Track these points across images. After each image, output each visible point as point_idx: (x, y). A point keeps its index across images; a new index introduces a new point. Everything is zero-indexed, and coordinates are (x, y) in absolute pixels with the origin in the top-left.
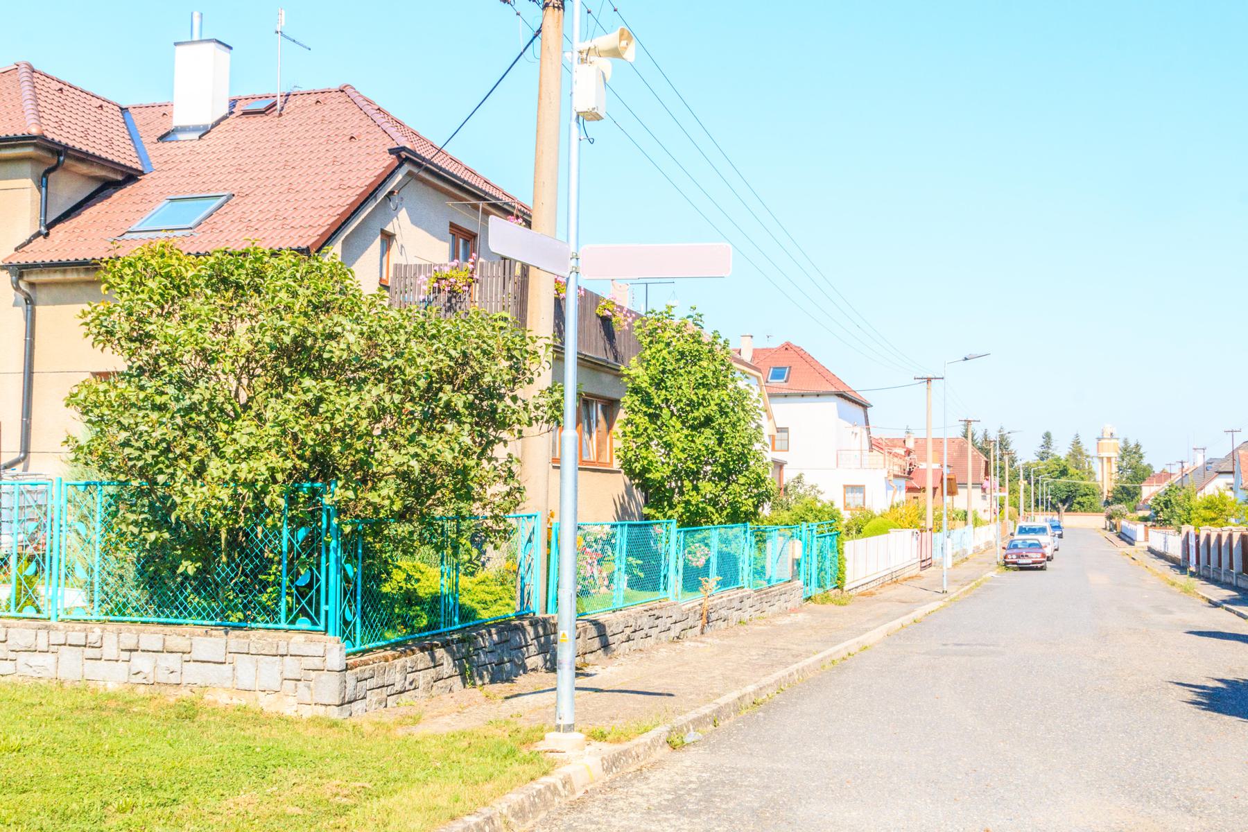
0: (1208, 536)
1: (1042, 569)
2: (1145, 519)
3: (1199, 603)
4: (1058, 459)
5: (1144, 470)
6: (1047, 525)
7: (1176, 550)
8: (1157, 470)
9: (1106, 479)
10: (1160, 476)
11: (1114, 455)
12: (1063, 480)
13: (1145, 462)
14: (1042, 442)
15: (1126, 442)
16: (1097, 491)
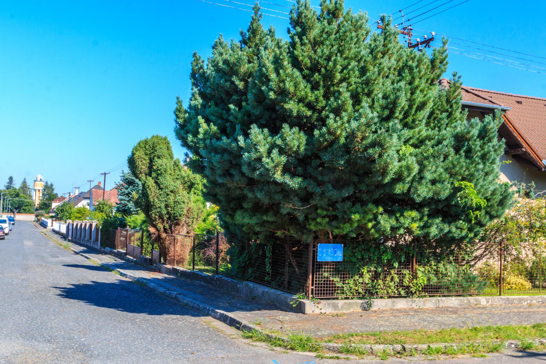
0: (77, 225)
1: (3, 239)
2: (52, 217)
3: (70, 252)
4: (16, 189)
5: (54, 196)
6: (7, 219)
7: (63, 230)
8: (59, 196)
9: (37, 199)
10: (60, 198)
11: (41, 188)
12: (17, 199)
13: (55, 192)
14: (8, 181)
15: (47, 183)
16: (32, 204)
